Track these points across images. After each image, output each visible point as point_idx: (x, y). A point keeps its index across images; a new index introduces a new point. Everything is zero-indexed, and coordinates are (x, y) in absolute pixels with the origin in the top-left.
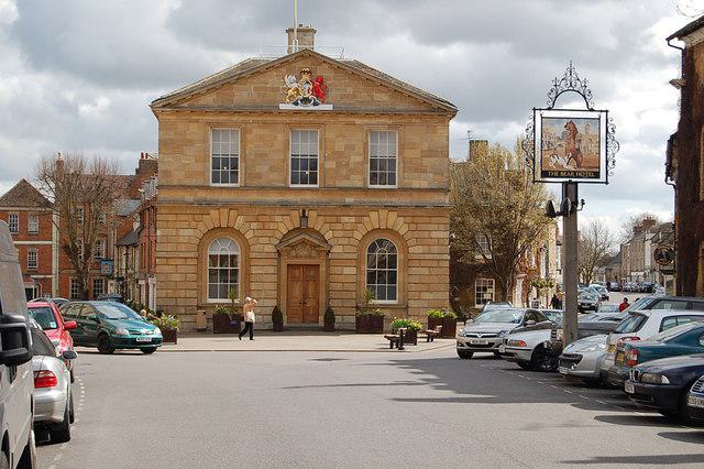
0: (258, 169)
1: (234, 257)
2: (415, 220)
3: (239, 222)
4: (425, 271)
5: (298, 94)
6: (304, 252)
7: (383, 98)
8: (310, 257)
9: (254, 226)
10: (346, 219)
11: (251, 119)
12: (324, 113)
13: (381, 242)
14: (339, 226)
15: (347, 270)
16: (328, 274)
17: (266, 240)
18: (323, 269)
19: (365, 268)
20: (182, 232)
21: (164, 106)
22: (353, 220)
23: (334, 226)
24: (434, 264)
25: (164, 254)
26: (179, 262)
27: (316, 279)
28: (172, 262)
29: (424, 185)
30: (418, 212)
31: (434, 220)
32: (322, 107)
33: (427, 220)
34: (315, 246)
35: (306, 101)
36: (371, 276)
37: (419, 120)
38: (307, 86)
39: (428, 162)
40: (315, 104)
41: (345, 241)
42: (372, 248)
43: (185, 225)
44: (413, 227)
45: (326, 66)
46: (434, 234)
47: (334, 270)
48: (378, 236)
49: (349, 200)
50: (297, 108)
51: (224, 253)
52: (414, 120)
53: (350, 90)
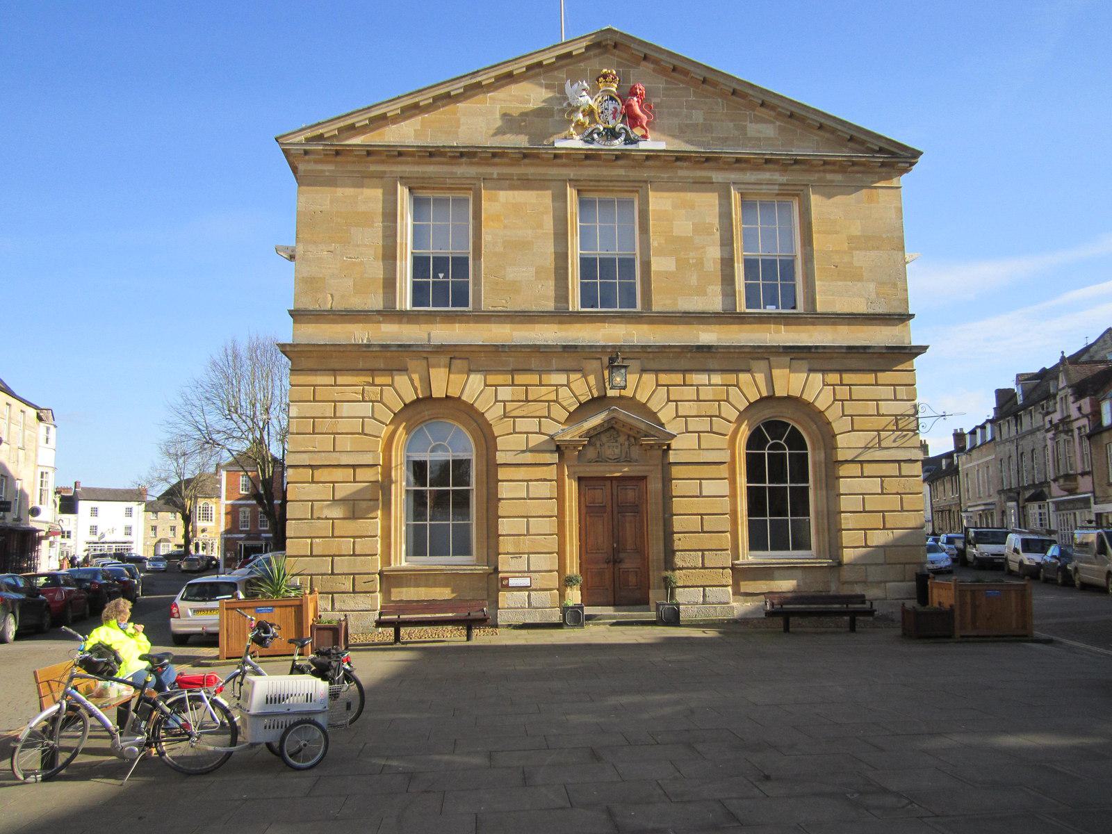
0: (511, 273)
1: (461, 467)
2: (848, 378)
3: (473, 388)
4: (874, 485)
5: (593, 121)
6: (612, 450)
7: (764, 135)
8: (628, 460)
9: (505, 393)
10: (702, 378)
11: (495, 171)
12: (652, 156)
13: (775, 427)
14: (690, 393)
15: (710, 488)
16: (667, 497)
17: (532, 425)
18: (654, 486)
19: (742, 481)
20: (345, 409)
21: (308, 140)
22: (717, 379)
23: (676, 393)
24: (892, 469)
25: (305, 459)
26: (339, 474)
27: (637, 509)
28: (321, 475)
29: (861, 307)
30: (853, 363)
31: (884, 377)
32: (643, 145)
33: (870, 378)
34: (634, 436)
35: (612, 134)
36: (756, 502)
37: (838, 177)
38: (611, 105)
39: (862, 259)
40: (629, 141)
41: (704, 425)
42: (755, 440)
43: (350, 393)
44: (843, 392)
45: (646, 67)
46: (885, 407)
47: (678, 487)
48: (768, 413)
49: (707, 336)
50: (591, 146)
51: (441, 456)
52: (829, 176)
53: (698, 117)
